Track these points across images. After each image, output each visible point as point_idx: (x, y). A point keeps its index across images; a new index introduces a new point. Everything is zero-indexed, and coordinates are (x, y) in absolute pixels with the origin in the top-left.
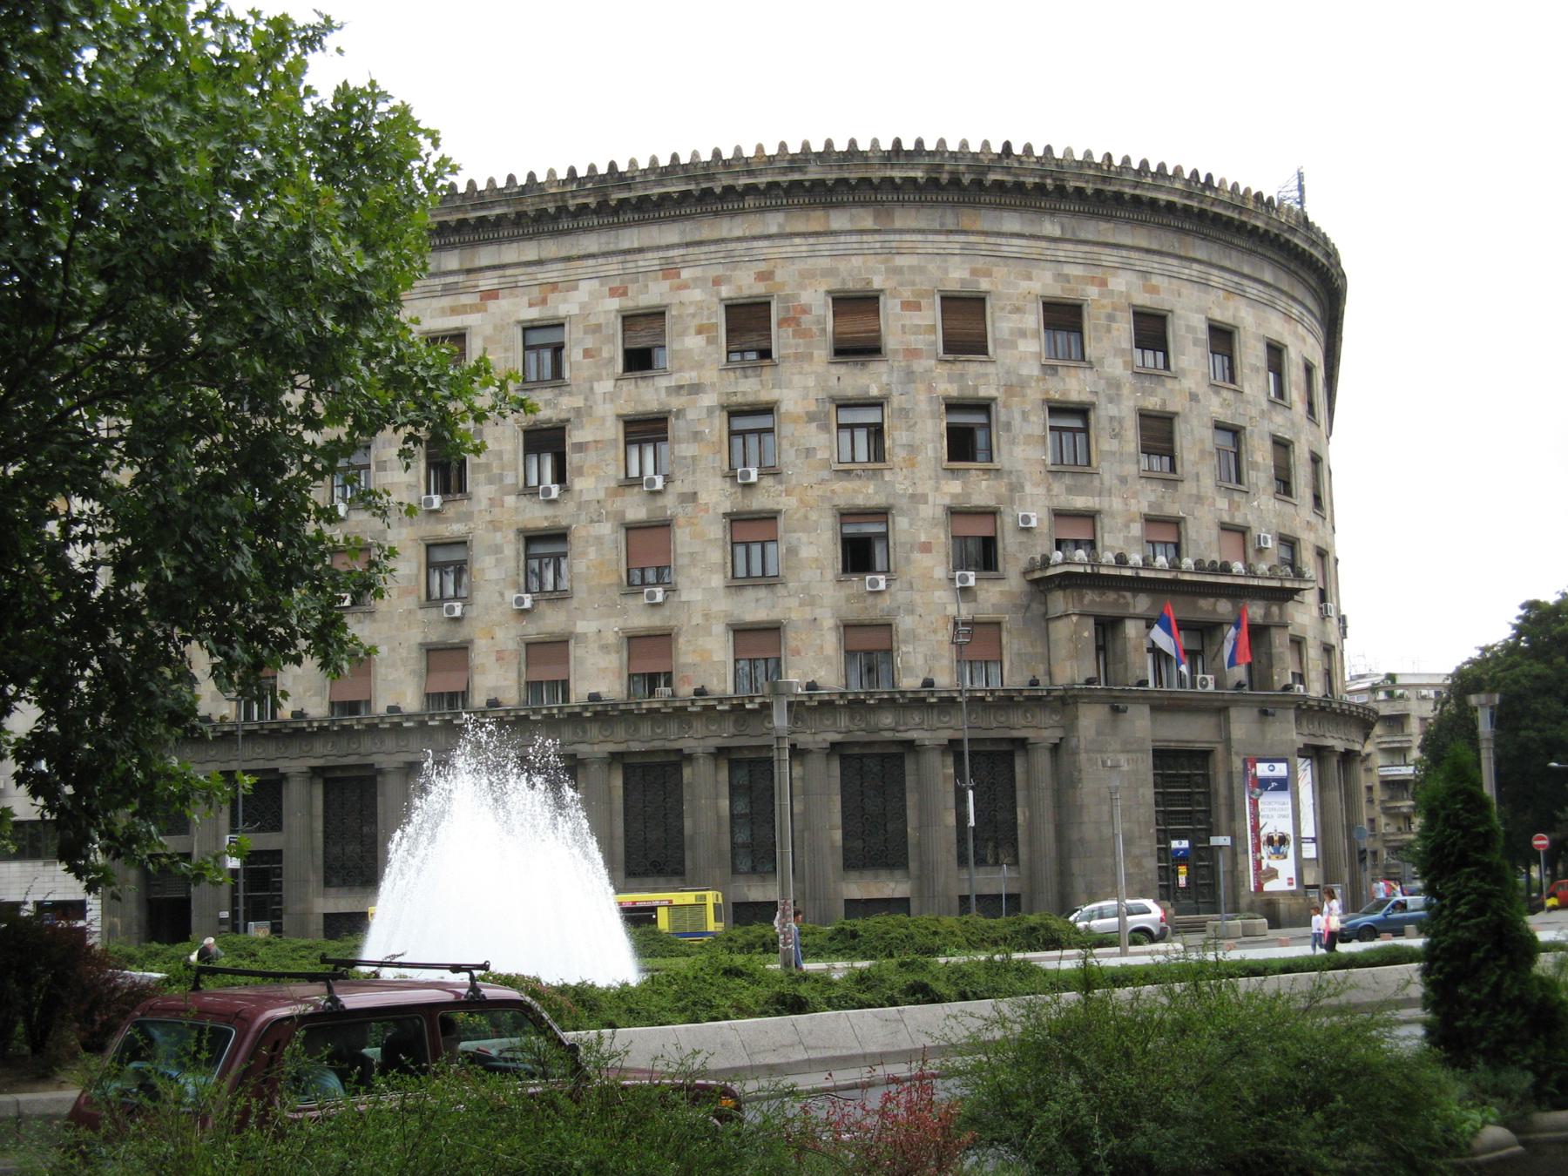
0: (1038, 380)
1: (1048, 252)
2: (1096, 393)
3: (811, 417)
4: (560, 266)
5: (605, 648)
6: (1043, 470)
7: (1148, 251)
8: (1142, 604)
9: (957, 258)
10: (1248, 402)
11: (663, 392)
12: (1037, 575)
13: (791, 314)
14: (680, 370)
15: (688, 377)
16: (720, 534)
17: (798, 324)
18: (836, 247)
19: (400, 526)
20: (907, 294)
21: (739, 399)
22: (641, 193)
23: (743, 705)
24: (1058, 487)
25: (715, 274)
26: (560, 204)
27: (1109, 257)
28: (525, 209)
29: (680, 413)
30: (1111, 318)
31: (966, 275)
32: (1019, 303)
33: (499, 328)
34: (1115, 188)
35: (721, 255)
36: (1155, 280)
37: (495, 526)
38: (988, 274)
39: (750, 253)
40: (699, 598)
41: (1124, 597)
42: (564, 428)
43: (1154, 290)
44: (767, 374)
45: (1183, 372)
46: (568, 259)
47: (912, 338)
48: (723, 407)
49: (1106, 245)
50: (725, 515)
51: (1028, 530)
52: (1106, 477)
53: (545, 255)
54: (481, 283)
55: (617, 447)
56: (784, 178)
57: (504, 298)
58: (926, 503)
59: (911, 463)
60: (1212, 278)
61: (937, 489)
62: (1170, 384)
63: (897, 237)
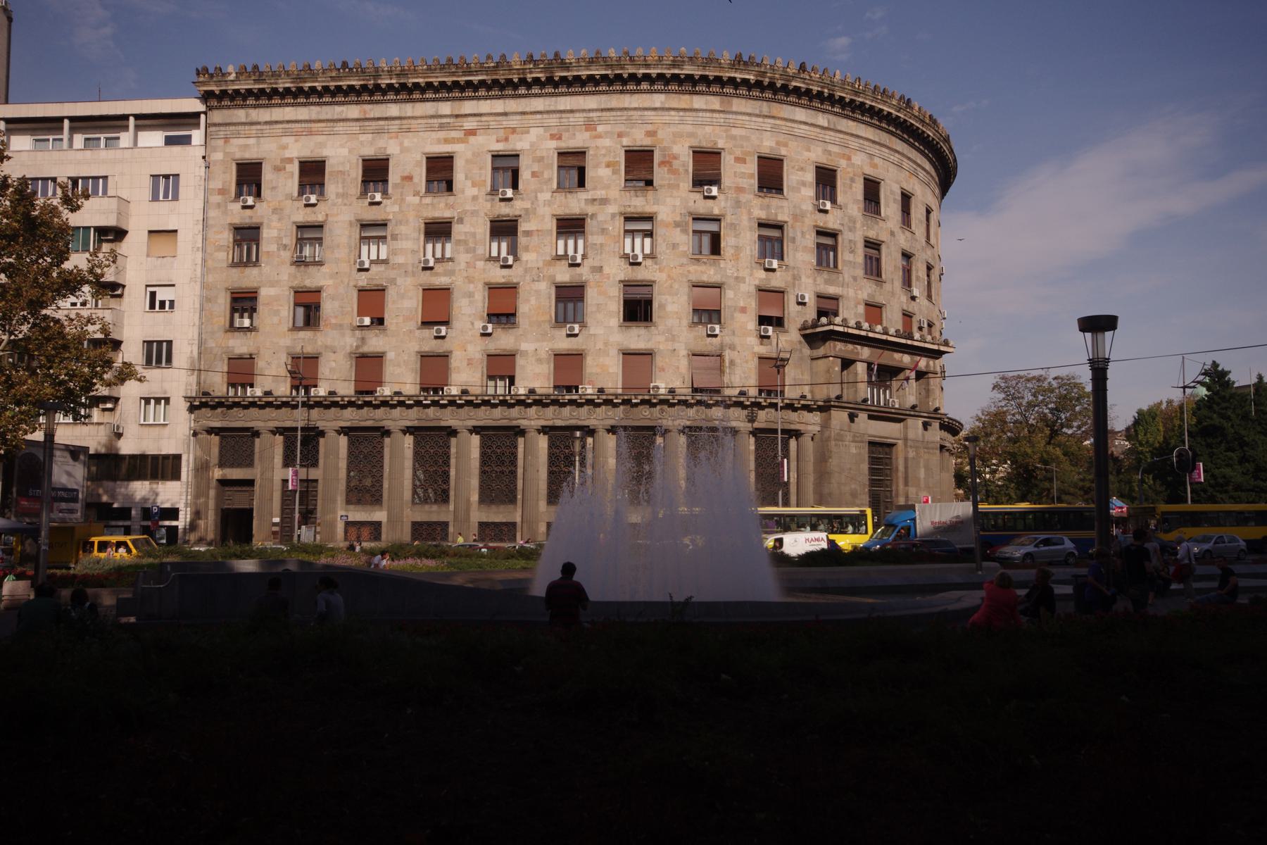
0: (811, 214)
1: (821, 136)
2: (843, 225)
3: (677, 225)
4: (518, 117)
5: (539, 361)
7: (874, 142)
8: (865, 352)
9: (769, 133)
10: (917, 240)
11: (583, 202)
12: (808, 331)
13: (667, 159)
14: (595, 189)
15: (600, 194)
16: (617, 295)
17: (671, 166)
18: (696, 119)
19: (406, 276)
20: (738, 153)
21: (631, 210)
22: (576, 73)
23: (630, 400)
24: (820, 280)
25: (619, 130)
26: (522, 76)
27: (854, 143)
28: (498, 77)
29: (593, 216)
30: (852, 180)
31: (773, 144)
32: (802, 165)
33: (476, 155)
34: (860, 100)
35: (624, 118)
37: (470, 280)
38: (786, 145)
39: (643, 118)
40: (602, 332)
41: (857, 349)
42: (517, 221)
43: (875, 166)
44: (650, 194)
45: (887, 217)
46: (523, 113)
47: (740, 180)
48: (621, 214)
49: (852, 135)
50: (621, 281)
51: (804, 304)
52: (846, 276)
53: (508, 110)
54: (465, 124)
55: (552, 235)
56: (668, 72)
57: (480, 135)
58: (745, 283)
59: (736, 257)
61: (751, 275)
62: (881, 223)
63: (734, 117)
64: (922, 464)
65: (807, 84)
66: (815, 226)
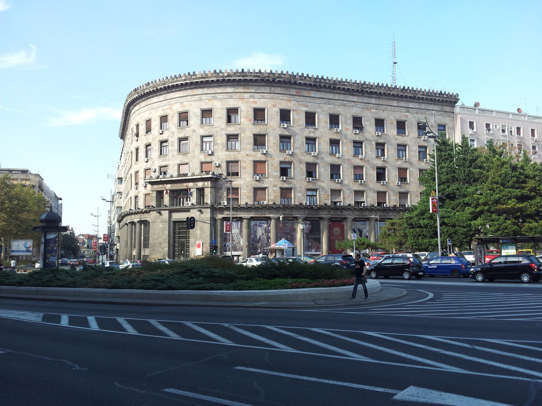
6: (158, 157)
8: (168, 186)
9: (147, 111)
24: (160, 161)
27: (173, 101)
30: (173, 117)
34: (167, 85)
36: (184, 104)
43: (184, 106)
49: (172, 99)
60: (203, 98)
64: (198, 229)
65: (149, 89)
66: (159, 141)
